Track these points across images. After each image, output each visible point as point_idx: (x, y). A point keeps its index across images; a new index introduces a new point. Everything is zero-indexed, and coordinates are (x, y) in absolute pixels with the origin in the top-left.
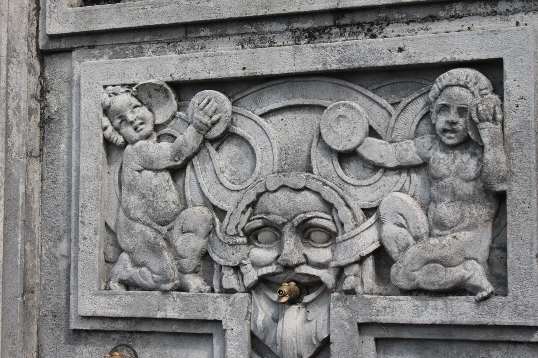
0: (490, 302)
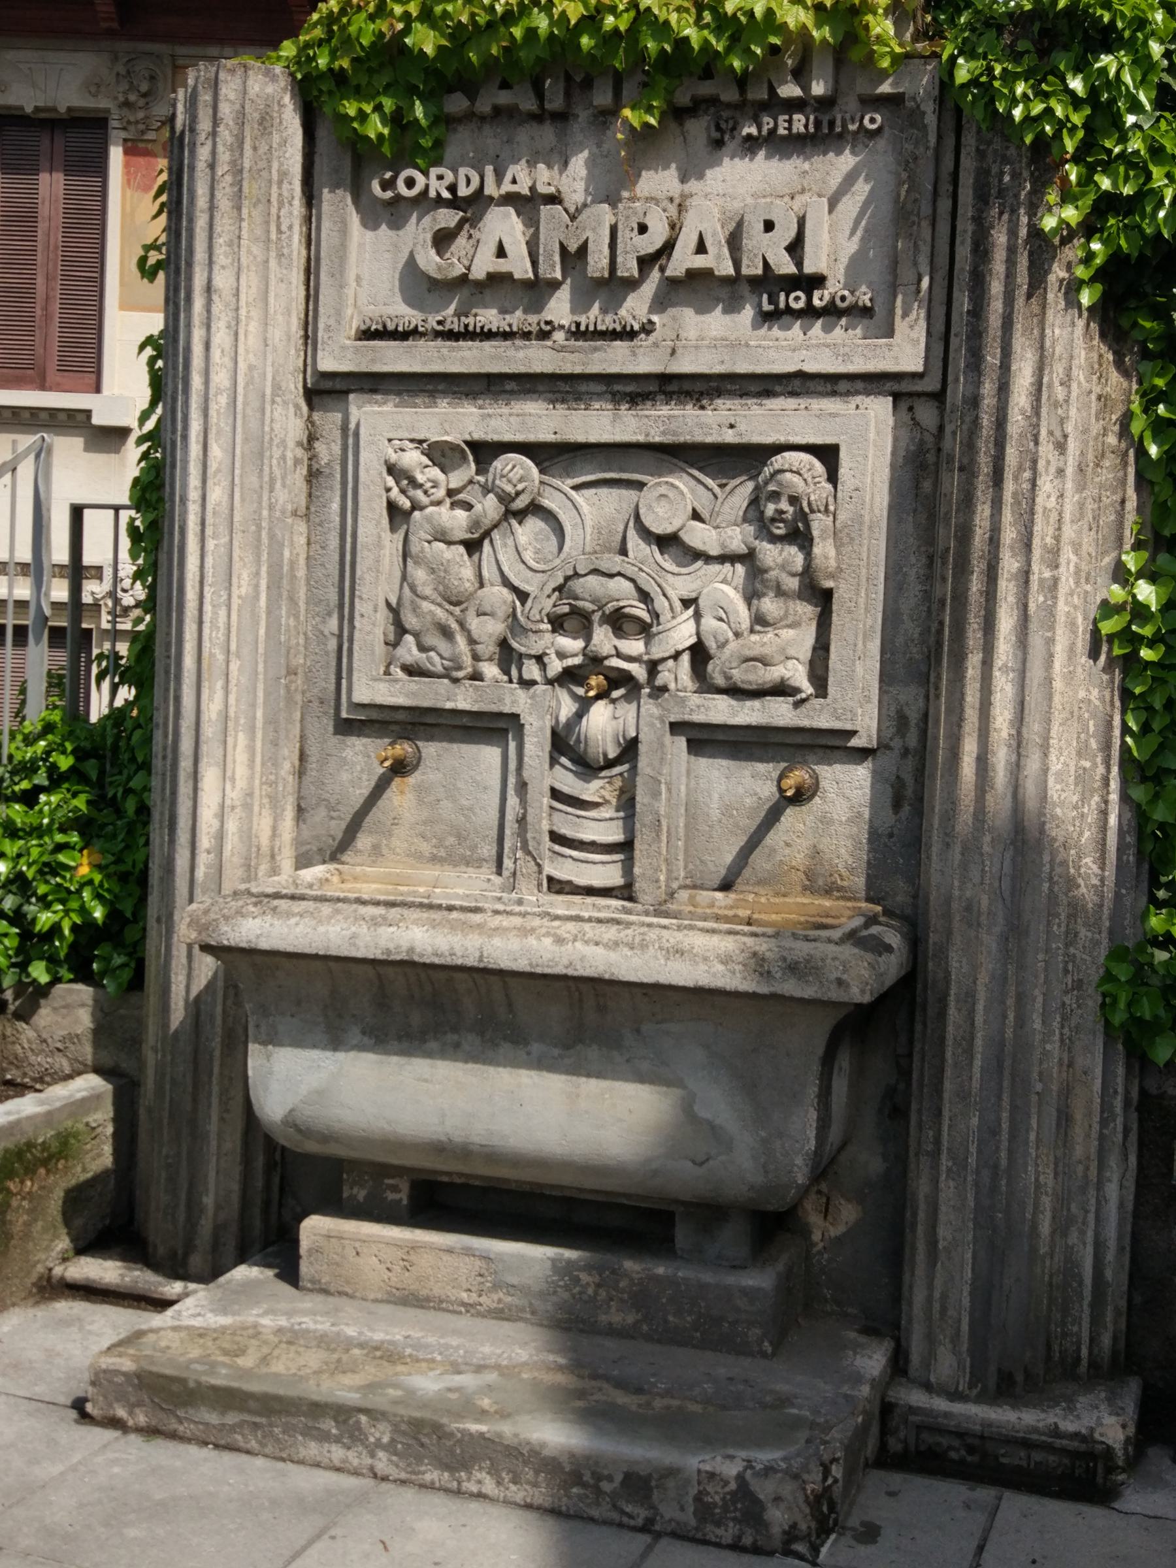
0: (807, 705)
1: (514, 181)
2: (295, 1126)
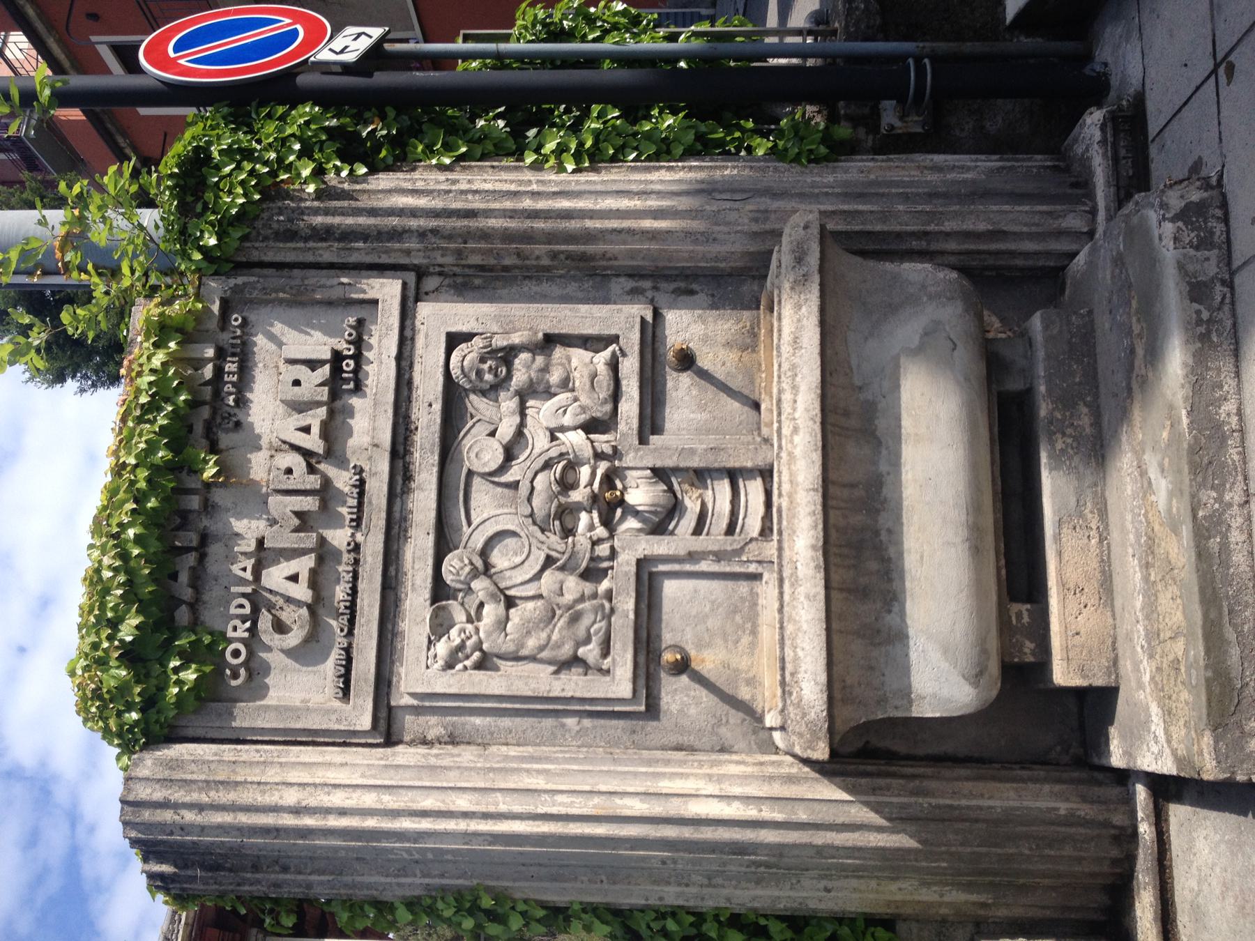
0: (624, 347)
1: (244, 569)
2: (980, 674)
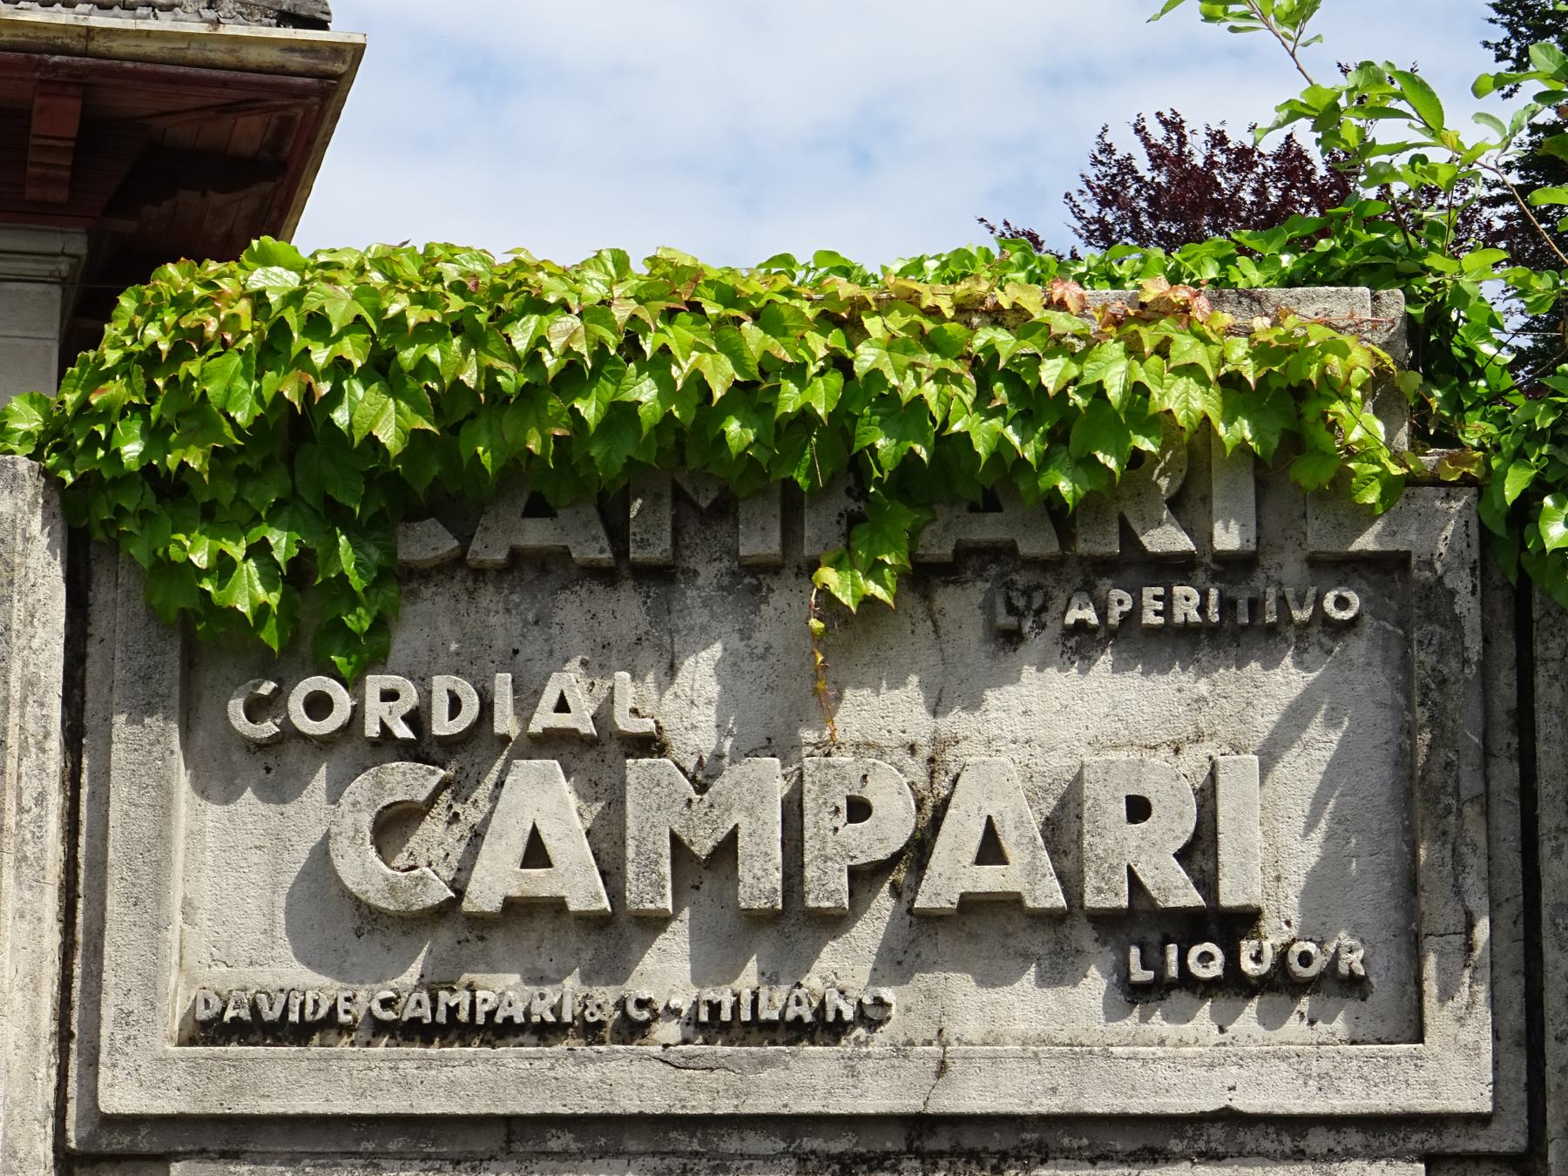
1: (562, 706)
